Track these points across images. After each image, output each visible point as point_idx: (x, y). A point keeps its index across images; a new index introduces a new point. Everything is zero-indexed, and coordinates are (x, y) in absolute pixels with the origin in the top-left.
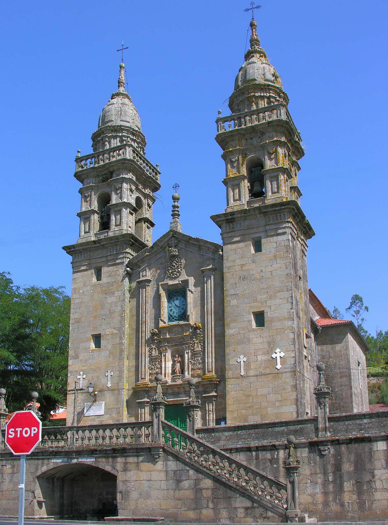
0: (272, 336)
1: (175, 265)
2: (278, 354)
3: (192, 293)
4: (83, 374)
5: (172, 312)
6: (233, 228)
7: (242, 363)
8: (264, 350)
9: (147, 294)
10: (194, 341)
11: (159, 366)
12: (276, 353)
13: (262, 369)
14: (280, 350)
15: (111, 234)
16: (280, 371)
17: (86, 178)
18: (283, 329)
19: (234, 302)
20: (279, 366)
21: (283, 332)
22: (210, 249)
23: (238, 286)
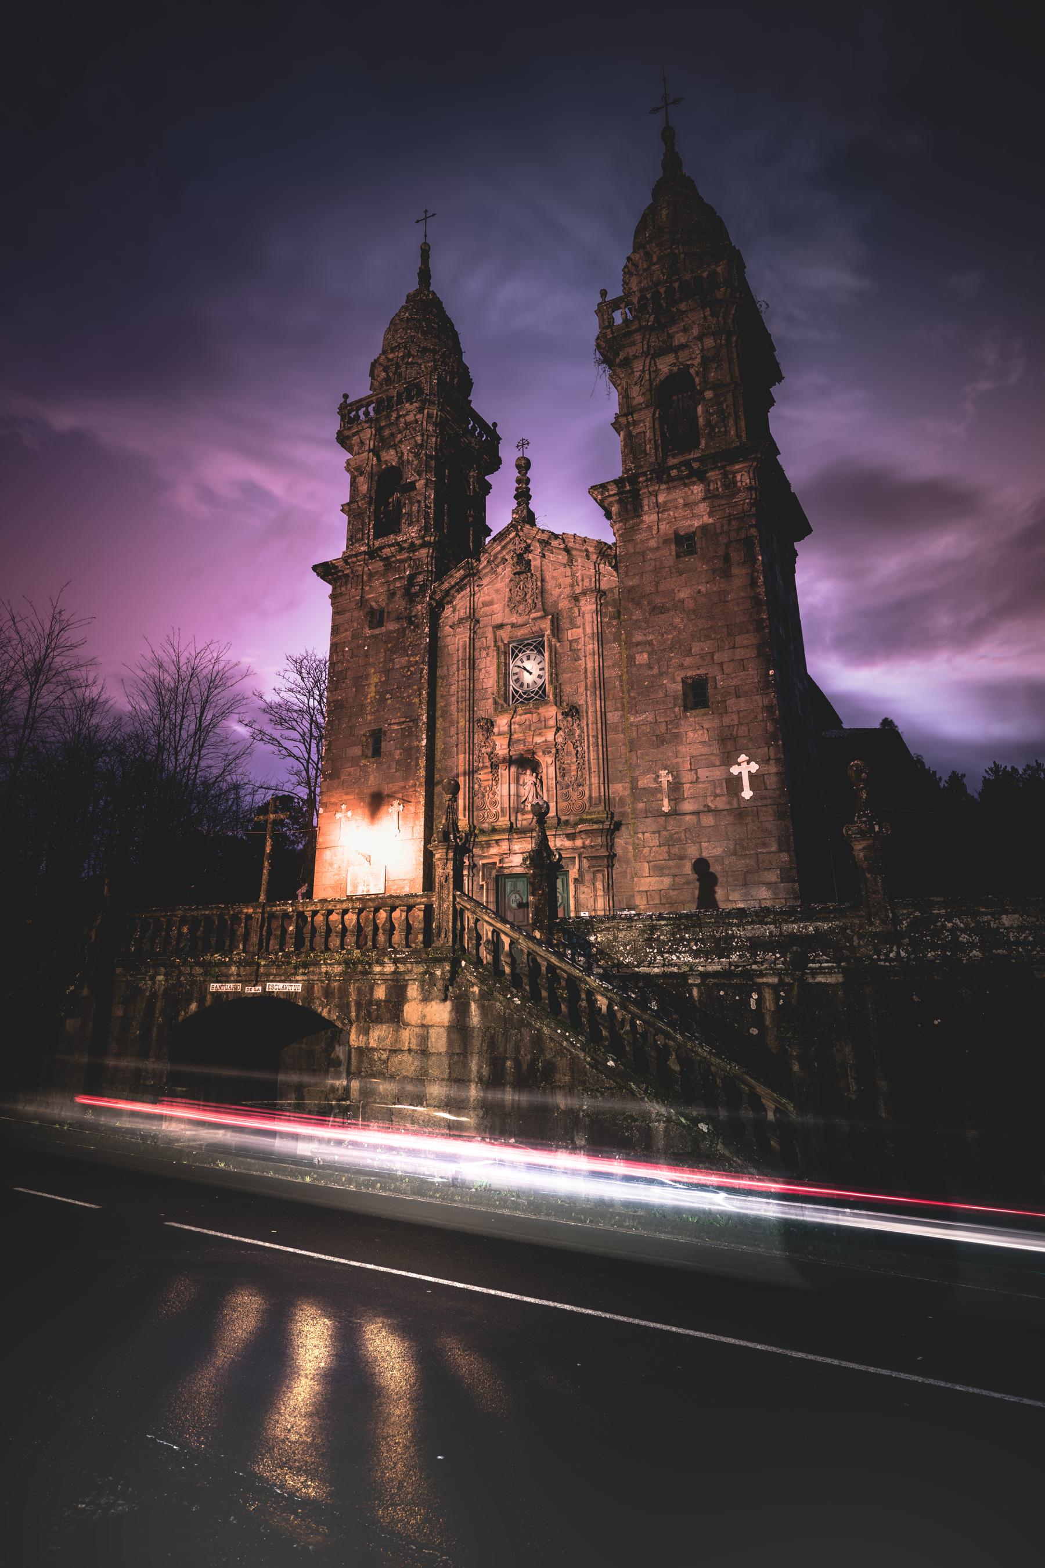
12: (739, 764)
14: (747, 758)
20: (747, 794)
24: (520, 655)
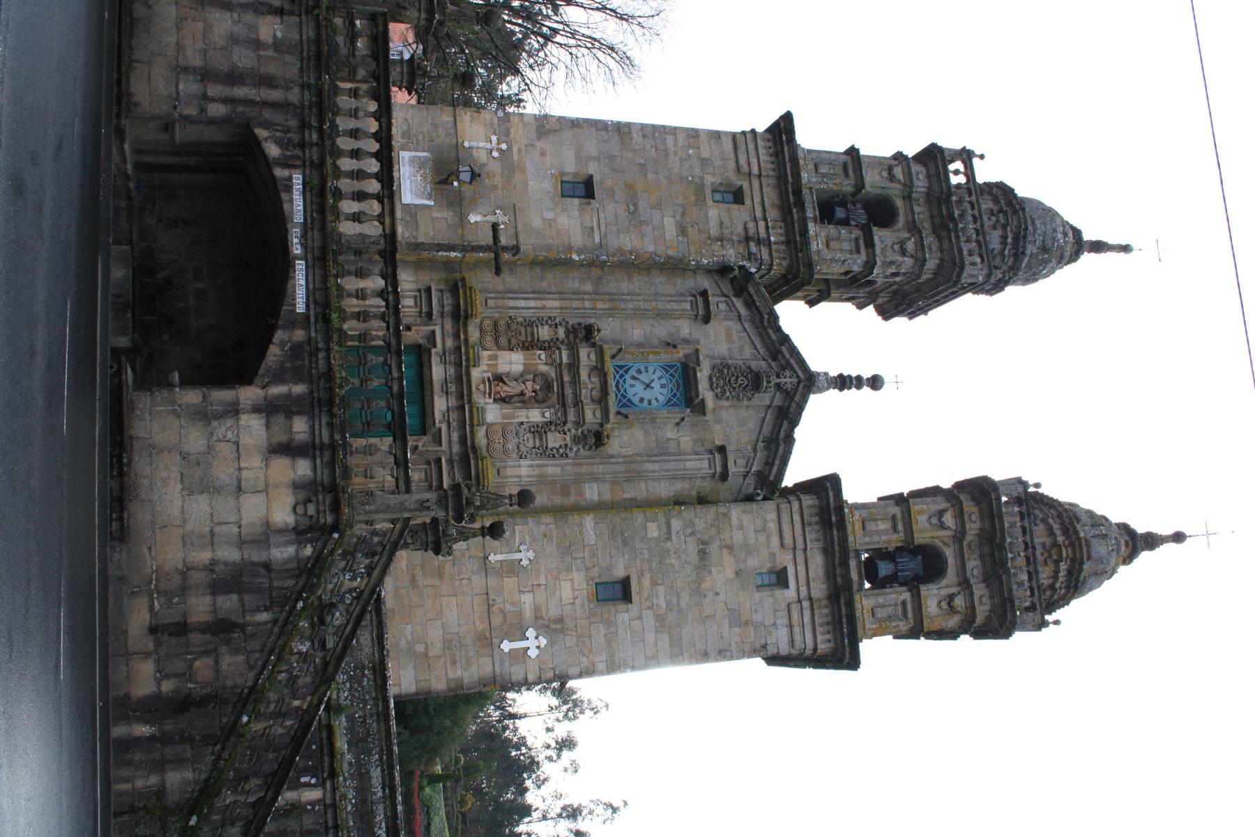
0: (576, 626)
1: (739, 382)
6: (810, 524)
7: (517, 556)
12: (536, 638)
13: (502, 605)
14: (542, 646)
15: (812, 228)
17: (928, 171)
18: (591, 651)
20: (506, 646)
21: (582, 652)
22: (768, 467)
23: (688, 539)
24: (668, 376)
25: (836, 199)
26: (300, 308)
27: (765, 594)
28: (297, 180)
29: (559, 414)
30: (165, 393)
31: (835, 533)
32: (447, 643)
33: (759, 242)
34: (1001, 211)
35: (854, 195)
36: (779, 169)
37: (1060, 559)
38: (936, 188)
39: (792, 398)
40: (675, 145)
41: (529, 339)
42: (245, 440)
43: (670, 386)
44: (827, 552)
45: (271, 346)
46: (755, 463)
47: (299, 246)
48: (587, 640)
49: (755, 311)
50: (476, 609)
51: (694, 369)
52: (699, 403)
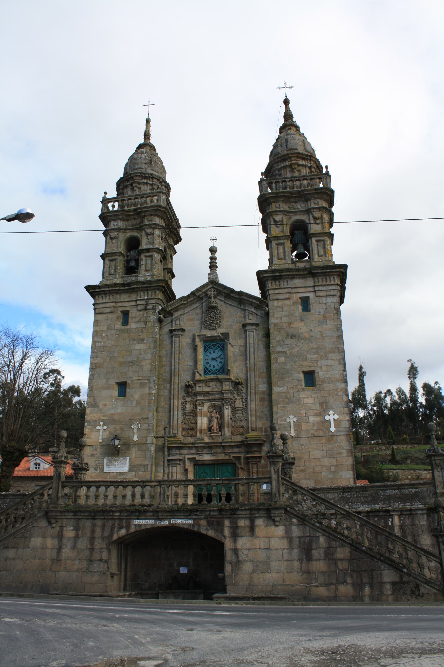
0: (325, 397)
1: (213, 316)
2: (332, 417)
3: (232, 346)
4: (104, 425)
5: (209, 365)
6: (280, 285)
7: (292, 423)
8: (316, 411)
9: (180, 344)
10: (234, 397)
11: (193, 422)
12: (329, 415)
13: (314, 431)
14: (333, 412)
15: (141, 279)
16: (335, 434)
17: (112, 220)
18: (336, 390)
19: (282, 359)
20: (333, 429)
22: (253, 304)
23: (285, 343)
24: (209, 350)
25: (126, 265)
26: (192, 522)
27: (311, 308)
28: (136, 522)
29: (227, 401)
30: (227, 579)
31: (284, 274)
32: (331, 456)
33: (147, 304)
34: (131, 185)
35: (124, 256)
36: (113, 293)
37: (297, 164)
38: (121, 217)
39: (221, 291)
40: (101, 342)
41: (192, 414)
42: (248, 546)
43: (214, 348)
44: (293, 277)
45: (208, 534)
46: (251, 310)
47: (165, 522)
48: (331, 392)
49: (180, 307)
50: (315, 443)
51: (206, 337)
52: (223, 336)
